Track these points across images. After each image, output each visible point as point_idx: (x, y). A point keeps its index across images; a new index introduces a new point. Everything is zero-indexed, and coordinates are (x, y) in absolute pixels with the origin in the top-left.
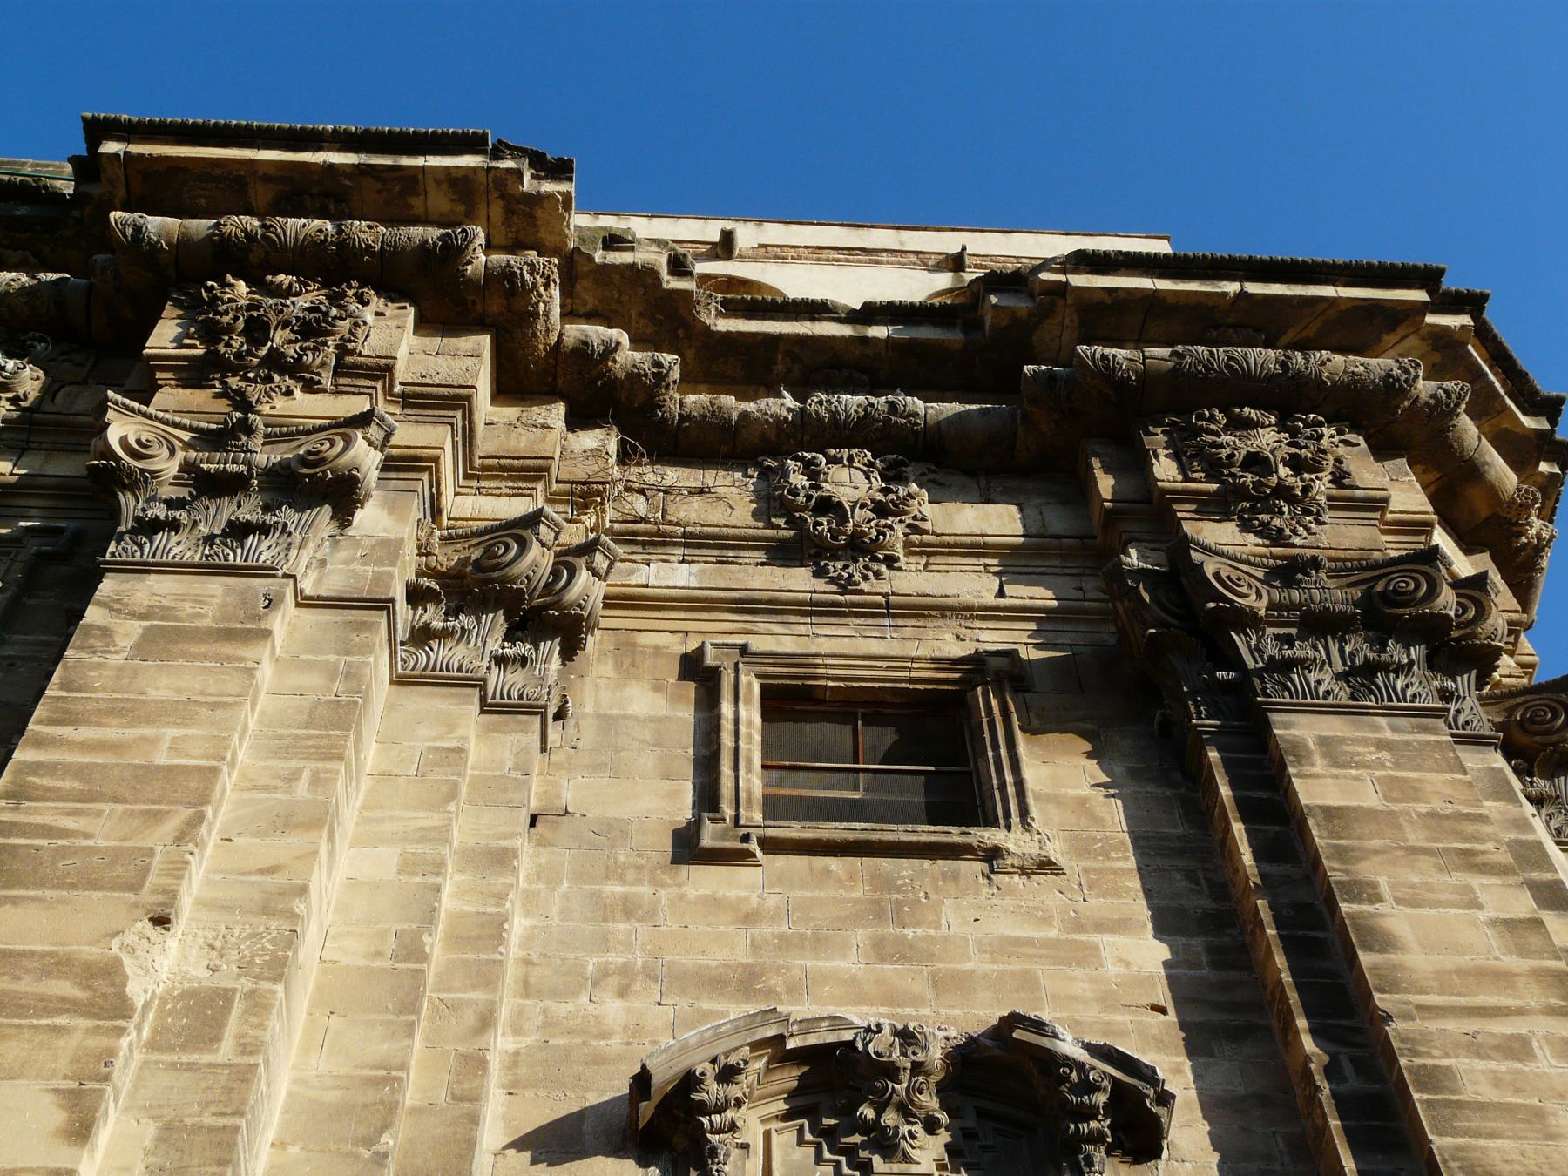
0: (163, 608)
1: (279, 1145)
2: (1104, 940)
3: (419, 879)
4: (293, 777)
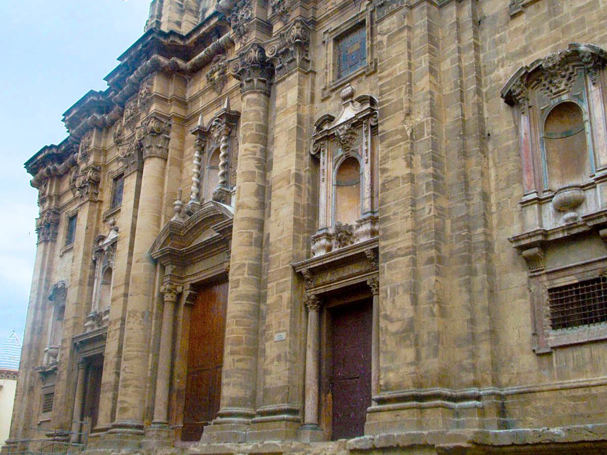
0: (388, 29)
1: (446, 142)
3: (454, 65)
4: (421, 63)
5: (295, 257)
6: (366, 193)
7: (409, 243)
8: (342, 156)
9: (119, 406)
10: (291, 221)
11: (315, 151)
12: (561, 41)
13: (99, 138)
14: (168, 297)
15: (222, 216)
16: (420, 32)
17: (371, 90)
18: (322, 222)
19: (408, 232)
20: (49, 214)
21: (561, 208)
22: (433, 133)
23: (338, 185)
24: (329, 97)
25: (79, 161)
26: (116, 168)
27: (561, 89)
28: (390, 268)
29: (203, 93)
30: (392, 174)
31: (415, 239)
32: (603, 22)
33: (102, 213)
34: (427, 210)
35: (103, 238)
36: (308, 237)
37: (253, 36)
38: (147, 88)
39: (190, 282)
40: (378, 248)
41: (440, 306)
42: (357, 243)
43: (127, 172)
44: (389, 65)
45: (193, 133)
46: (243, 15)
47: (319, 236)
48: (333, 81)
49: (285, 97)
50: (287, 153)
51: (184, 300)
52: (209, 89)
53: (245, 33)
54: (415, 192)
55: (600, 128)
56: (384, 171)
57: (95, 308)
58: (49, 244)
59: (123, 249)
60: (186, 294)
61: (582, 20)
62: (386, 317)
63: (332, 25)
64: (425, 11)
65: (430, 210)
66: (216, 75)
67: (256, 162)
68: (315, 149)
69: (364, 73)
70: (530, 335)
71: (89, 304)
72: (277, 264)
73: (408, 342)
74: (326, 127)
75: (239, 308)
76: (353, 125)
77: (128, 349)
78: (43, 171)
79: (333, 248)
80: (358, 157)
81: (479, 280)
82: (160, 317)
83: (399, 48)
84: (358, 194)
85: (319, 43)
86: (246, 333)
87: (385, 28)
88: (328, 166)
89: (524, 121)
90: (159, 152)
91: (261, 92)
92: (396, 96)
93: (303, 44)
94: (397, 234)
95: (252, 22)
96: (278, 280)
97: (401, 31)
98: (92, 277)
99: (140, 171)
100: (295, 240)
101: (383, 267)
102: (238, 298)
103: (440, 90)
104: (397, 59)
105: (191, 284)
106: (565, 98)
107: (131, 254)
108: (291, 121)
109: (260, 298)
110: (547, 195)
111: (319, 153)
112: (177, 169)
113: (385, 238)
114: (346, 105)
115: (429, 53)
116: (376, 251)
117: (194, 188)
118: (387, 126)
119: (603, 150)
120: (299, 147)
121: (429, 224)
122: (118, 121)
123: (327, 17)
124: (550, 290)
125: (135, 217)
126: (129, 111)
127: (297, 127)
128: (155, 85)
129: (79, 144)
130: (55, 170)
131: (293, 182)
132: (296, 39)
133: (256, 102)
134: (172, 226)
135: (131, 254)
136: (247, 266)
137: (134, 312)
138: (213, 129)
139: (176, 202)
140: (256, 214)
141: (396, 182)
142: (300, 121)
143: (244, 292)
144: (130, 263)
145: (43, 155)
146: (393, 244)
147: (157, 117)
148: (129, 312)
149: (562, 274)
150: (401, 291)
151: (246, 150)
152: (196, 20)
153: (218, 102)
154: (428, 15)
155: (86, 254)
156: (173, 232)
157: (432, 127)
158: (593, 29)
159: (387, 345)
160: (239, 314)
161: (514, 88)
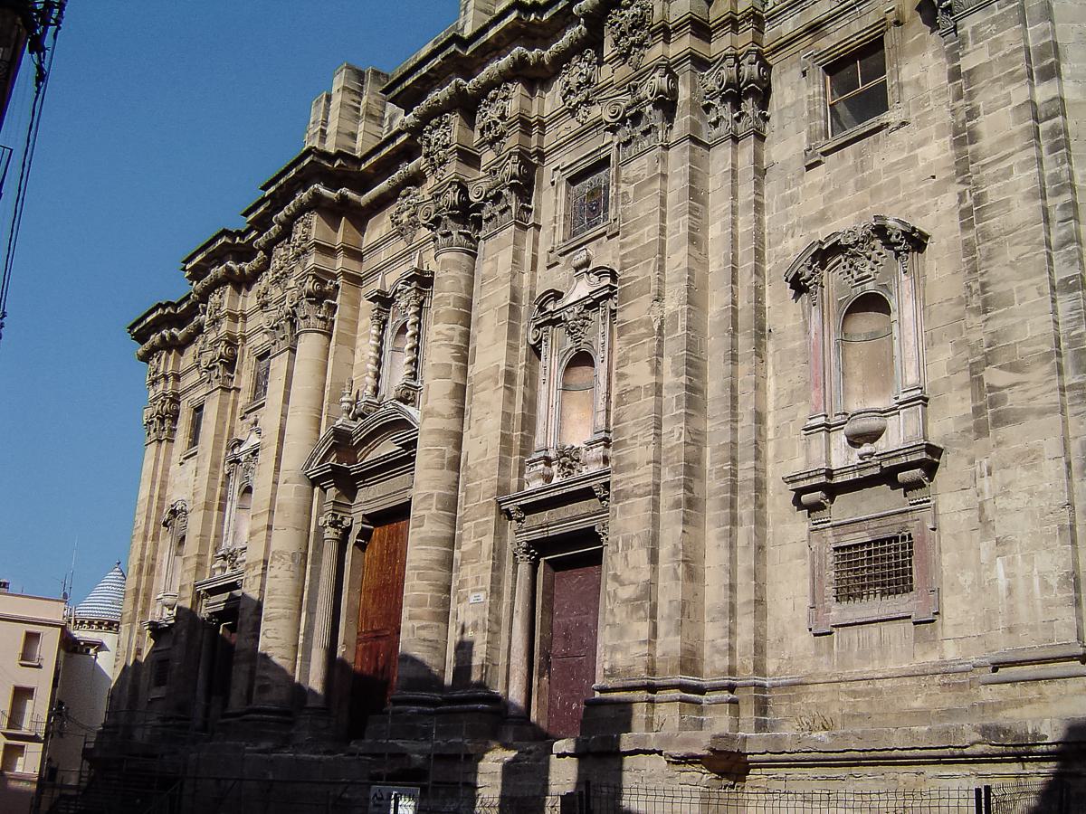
2: (918, 151)
5: (502, 489)
6: (601, 406)
7: (650, 480)
8: (571, 348)
9: (257, 683)
10: (497, 438)
11: (535, 340)
12: (869, 208)
13: (234, 300)
14: (330, 533)
15: (404, 424)
16: (677, 184)
17: (613, 257)
18: (539, 441)
19: (648, 463)
20: (163, 402)
21: (855, 440)
22: (689, 328)
23: (566, 388)
24: (557, 264)
25: (206, 329)
26: (259, 341)
27: (864, 274)
28: (624, 511)
29: (385, 240)
30: (632, 382)
31: (657, 473)
32: (922, 187)
33: (240, 406)
34: (677, 435)
35: (240, 443)
36: (521, 461)
37: (452, 169)
38: (303, 232)
39: (363, 512)
40: (609, 482)
41: (687, 565)
42: (585, 472)
43: (274, 350)
44: (633, 228)
45: (369, 300)
46: (438, 139)
47: (535, 460)
48: (564, 241)
49: (495, 260)
50: (496, 341)
51: (352, 538)
52: (395, 235)
53: (441, 164)
54: (659, 409)
55: (910, 334)
56: (621, 376)
57: (227, 544)
58: (164, 443)
59: (266, 459)
60: (356, 529)
61: (896, 181)
62: (616, 578)
63: (565, 158)
64: (687, 153)
65: (681, 434)
66: (404, 217)
67: (453, 351)
68: (535, 337)
69: (605, 233)
70: (807, 609)
71: (219, 536)
72: (478, 497)
73: (642, 613)
74: (550, 307)
75: (423, 555)
76: (588, 307)
77: (271, 604)
78: (155, 338)
79: (555, 477)
80: (592, 353)
81: (744, 532)
82: (317, 560)
83: (646, 206)
84: (593, 403)
85: (546, 182)
86: (433, 590)
87: (631, 175)
88: (552, 363)
89: (815, 316)
90: (320, 324)
91: (464, 251)
92: (641, 273)
93: (525, 187)
94: (633, 466)
95: (450, 149)
96: (477, 518)
97: (652, 180)
98: (223, 498)
99: (293, 350)
100: (503, 464)
101: (614, 509)
102: (422, 541)
103: (705, 265)
104: (646, 220)
105: (364, 515)
106: (870, 287)
107: (277, 469)
108: (503, 296)
109: (451, 542)
110: (839, 419)
111: (540, 342)
112: (347, 349)
113: (618, 470)
114: (579, 277)
115: (690, 213)
116: (607, 486)
117: (370, 381)
118: (629, 314)
119: (911, 363)
120: (513, 332)
121: (678, 454)
122: (264, 274)
123: (559, 147)
124: (836, 549)
125: (284, 415)
126: (278, 262)
127: (510, 305)
128: (314, 227)
129: (207, 303)
130: (173, 337)
131: (501, 383)
132: (511, 180)
133: (457, 266)
134: (338, 433)
135: (277, 469)
136: (435, 497)
137: (281, 553)
138: (398, 295)
139: (344, 399)
140: (452, 425)
141: (636, 393)
142: (515, 297)
143: (430, 534)
144: (275, 482)
145: (154, 315)
146: (630, 478)
147: (320, 276)
148: (273, 552)
149: (850, 528)
150: (636, 542)
151: (438, 333)
152: (380, 129)
153: (407, 253)
154: (691, 160)
155: (215, 465)
156: (341, 440)
157: (689, 320)
158: (910, 196)
159: (614, 615)
160: (422, 564)
161: (803, 269)
